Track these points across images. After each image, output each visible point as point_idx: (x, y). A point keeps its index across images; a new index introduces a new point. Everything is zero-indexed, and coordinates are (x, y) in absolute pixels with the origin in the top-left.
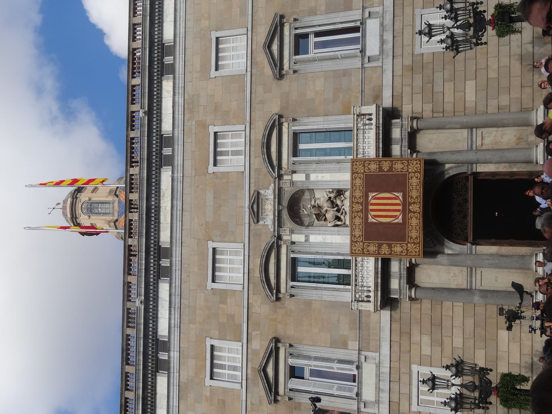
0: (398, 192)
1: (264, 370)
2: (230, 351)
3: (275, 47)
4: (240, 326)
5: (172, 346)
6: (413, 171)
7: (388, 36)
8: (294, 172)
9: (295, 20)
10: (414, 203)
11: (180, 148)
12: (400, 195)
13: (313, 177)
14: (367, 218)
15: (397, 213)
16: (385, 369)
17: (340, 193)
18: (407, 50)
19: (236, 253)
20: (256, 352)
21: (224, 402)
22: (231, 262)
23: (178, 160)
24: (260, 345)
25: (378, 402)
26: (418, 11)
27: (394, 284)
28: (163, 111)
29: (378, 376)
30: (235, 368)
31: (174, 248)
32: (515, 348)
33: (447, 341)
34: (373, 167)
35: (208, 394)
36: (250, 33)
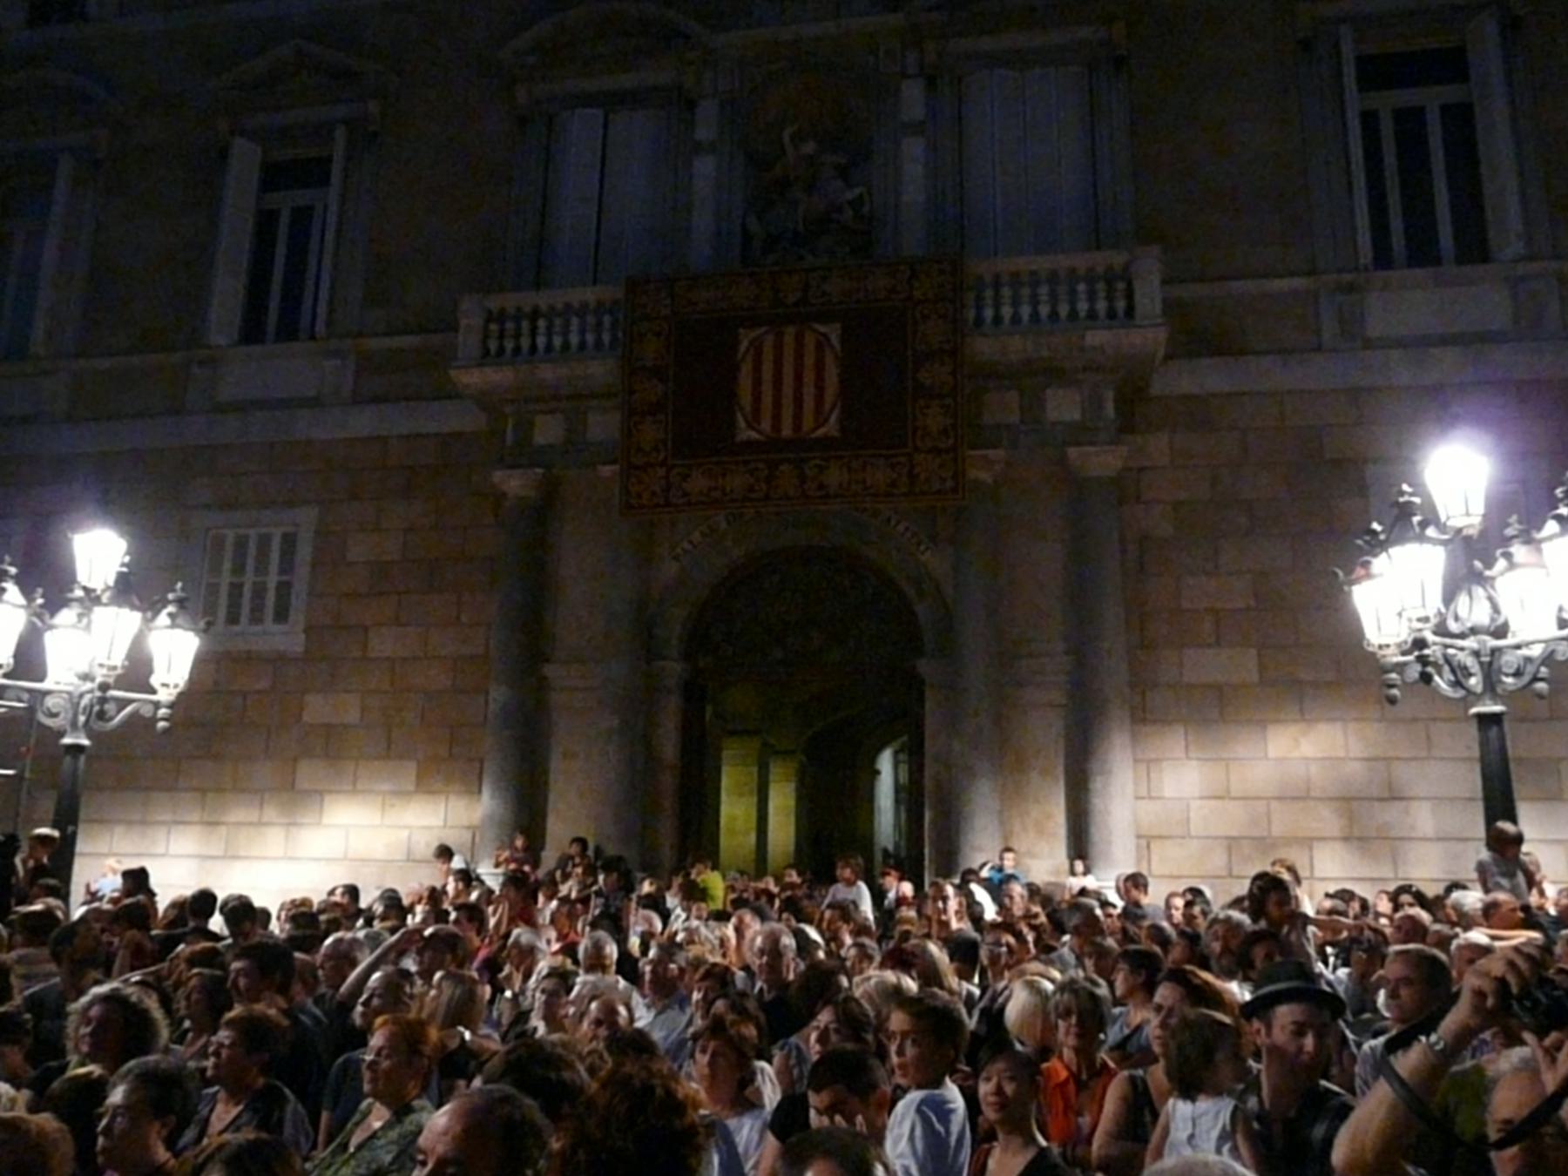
6: (916, 471)
8: (931, 82)
10: (803, 479)
12: (831, 428)
15: (766, 425)
29: (285, 404)
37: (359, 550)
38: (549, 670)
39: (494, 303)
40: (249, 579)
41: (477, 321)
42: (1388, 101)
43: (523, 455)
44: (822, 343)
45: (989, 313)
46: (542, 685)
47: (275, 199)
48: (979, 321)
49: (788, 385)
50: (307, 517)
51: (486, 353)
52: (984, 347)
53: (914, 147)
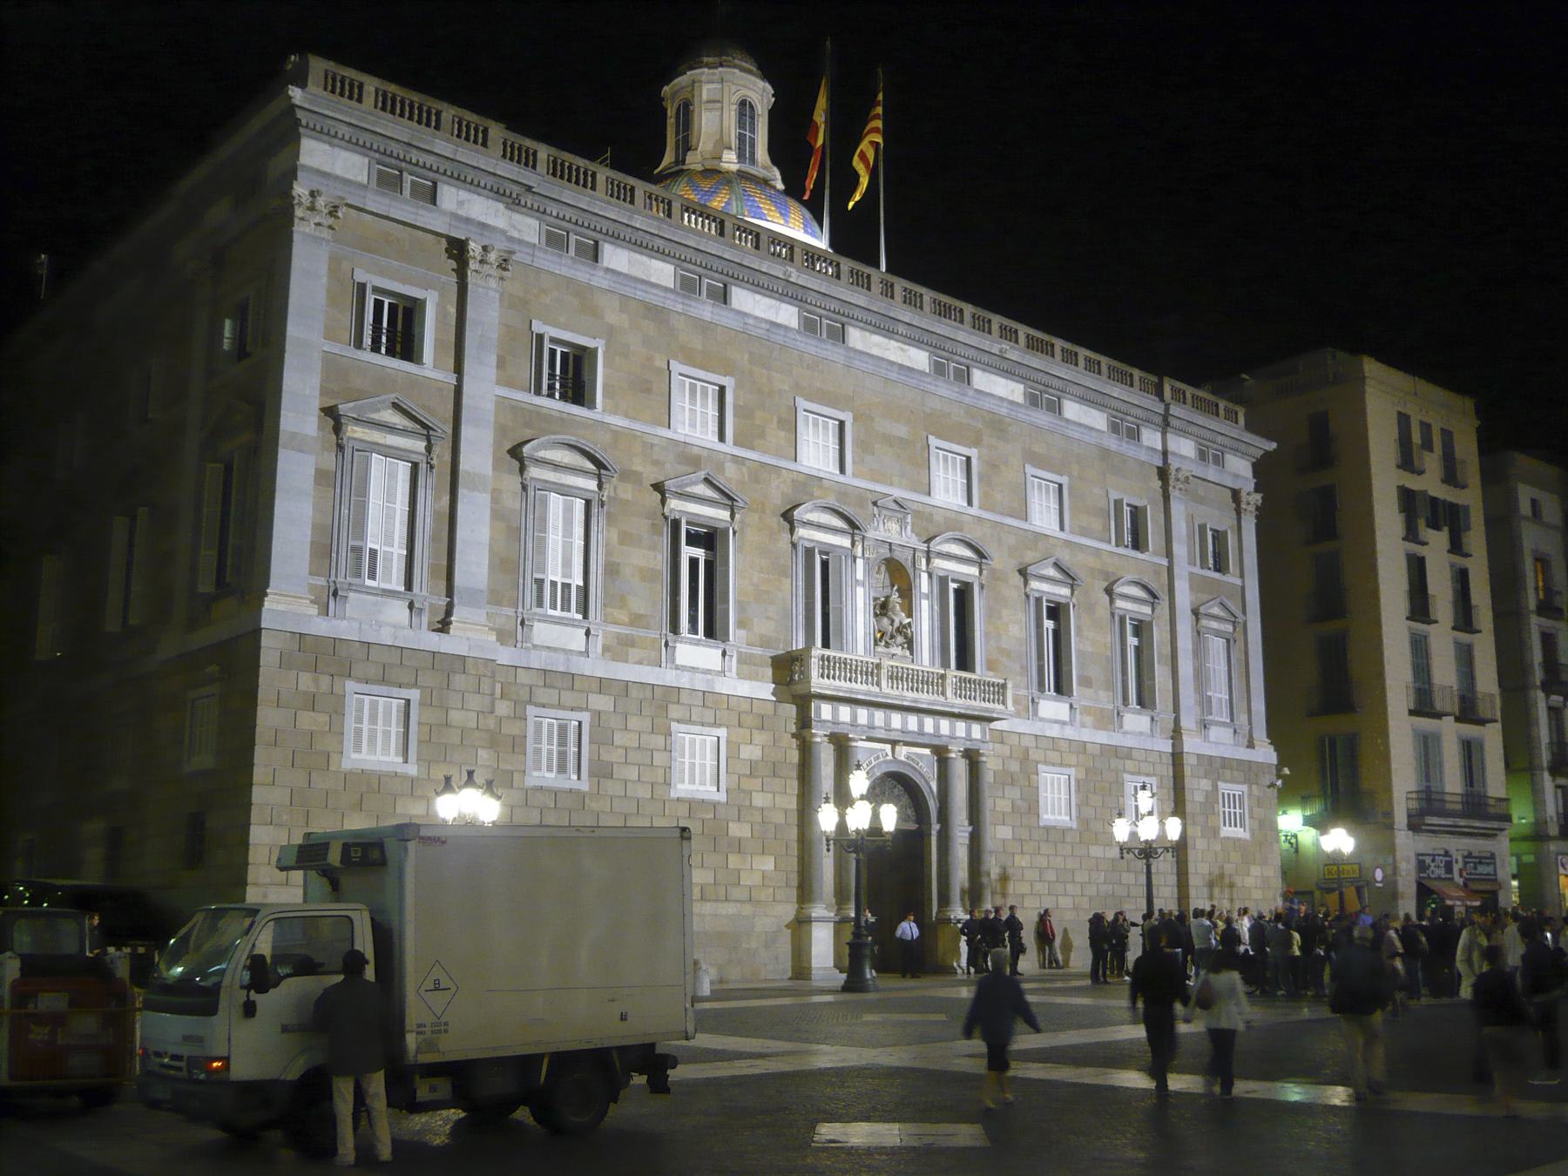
3: (1051, 572)
4: (752, 448)
5: (716, 310)
7: (1054, 731)
8: (930, 576)
11: (954, 396)
17: (910, 644)
20: (720, 467)
21: (648, 391)
24: (730, 477)
25: (677, 668)
26: (1072, 771)
27: (826, 711)
28: (994, 378)
29: (707, 672)
31: (842, 351)
32: (756, 879)
35: (657, 363)
53: (925, 603)
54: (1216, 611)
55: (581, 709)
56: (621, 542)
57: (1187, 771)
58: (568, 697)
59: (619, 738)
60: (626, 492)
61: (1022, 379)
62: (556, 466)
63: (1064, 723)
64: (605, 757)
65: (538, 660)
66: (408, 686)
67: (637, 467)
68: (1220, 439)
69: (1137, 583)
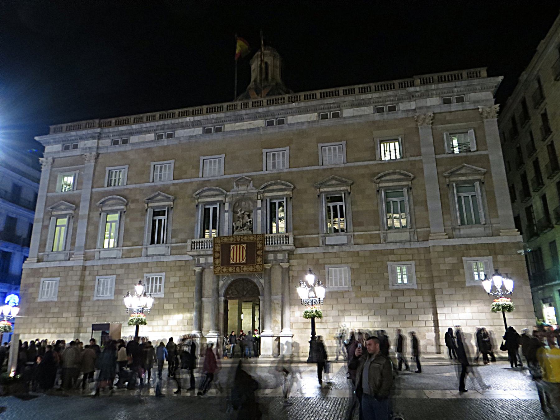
0: (246, 260)
1: (159, 194)
2: (169, 174)
3: (334, 182)
8: (262, 201)
9: (349, 193)
13: (259, 212)
14: (233, 244)
15: (235, 261)
16: (163, 259)
18: (327, 261)
19: (219, 172)
22: (215, 169)
23: (270, 130)
25: (147, 256)
29: (159, 255)
30: (160, 178)
33: (177, 289)
34: (259, 246)
36: (343, 165)
37: (172, 280)
38: (203, 299)
39: (193, 240)
40: (154, 285)
41: (190, 244)
42: (331, 205)
43: (199, 265)
44: (243, 247)
45: (268, 243)
46: (202, 302)
47: (156, 218)
48: (267, 244)
49: (238, 254)
50: (164, 274)
51: (192, 248)
52: (267, 249)
54: (463, 171)
55: (113, 274)
56: (130, 221)
57: (433, 255)
58: (110, 272)
59: (125, 282)
60: (132, 206)
61: (314, 111)
62: (110, 206)
63: (343, 245)
64: (120, 288)
65: (100, 263)
66: (57, 277)
67: (137, 198)
68: (456, 89)
69: (394, 173)
